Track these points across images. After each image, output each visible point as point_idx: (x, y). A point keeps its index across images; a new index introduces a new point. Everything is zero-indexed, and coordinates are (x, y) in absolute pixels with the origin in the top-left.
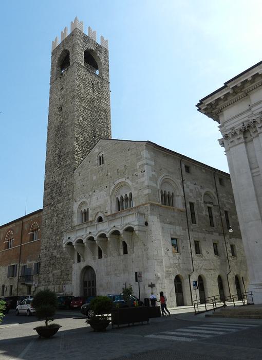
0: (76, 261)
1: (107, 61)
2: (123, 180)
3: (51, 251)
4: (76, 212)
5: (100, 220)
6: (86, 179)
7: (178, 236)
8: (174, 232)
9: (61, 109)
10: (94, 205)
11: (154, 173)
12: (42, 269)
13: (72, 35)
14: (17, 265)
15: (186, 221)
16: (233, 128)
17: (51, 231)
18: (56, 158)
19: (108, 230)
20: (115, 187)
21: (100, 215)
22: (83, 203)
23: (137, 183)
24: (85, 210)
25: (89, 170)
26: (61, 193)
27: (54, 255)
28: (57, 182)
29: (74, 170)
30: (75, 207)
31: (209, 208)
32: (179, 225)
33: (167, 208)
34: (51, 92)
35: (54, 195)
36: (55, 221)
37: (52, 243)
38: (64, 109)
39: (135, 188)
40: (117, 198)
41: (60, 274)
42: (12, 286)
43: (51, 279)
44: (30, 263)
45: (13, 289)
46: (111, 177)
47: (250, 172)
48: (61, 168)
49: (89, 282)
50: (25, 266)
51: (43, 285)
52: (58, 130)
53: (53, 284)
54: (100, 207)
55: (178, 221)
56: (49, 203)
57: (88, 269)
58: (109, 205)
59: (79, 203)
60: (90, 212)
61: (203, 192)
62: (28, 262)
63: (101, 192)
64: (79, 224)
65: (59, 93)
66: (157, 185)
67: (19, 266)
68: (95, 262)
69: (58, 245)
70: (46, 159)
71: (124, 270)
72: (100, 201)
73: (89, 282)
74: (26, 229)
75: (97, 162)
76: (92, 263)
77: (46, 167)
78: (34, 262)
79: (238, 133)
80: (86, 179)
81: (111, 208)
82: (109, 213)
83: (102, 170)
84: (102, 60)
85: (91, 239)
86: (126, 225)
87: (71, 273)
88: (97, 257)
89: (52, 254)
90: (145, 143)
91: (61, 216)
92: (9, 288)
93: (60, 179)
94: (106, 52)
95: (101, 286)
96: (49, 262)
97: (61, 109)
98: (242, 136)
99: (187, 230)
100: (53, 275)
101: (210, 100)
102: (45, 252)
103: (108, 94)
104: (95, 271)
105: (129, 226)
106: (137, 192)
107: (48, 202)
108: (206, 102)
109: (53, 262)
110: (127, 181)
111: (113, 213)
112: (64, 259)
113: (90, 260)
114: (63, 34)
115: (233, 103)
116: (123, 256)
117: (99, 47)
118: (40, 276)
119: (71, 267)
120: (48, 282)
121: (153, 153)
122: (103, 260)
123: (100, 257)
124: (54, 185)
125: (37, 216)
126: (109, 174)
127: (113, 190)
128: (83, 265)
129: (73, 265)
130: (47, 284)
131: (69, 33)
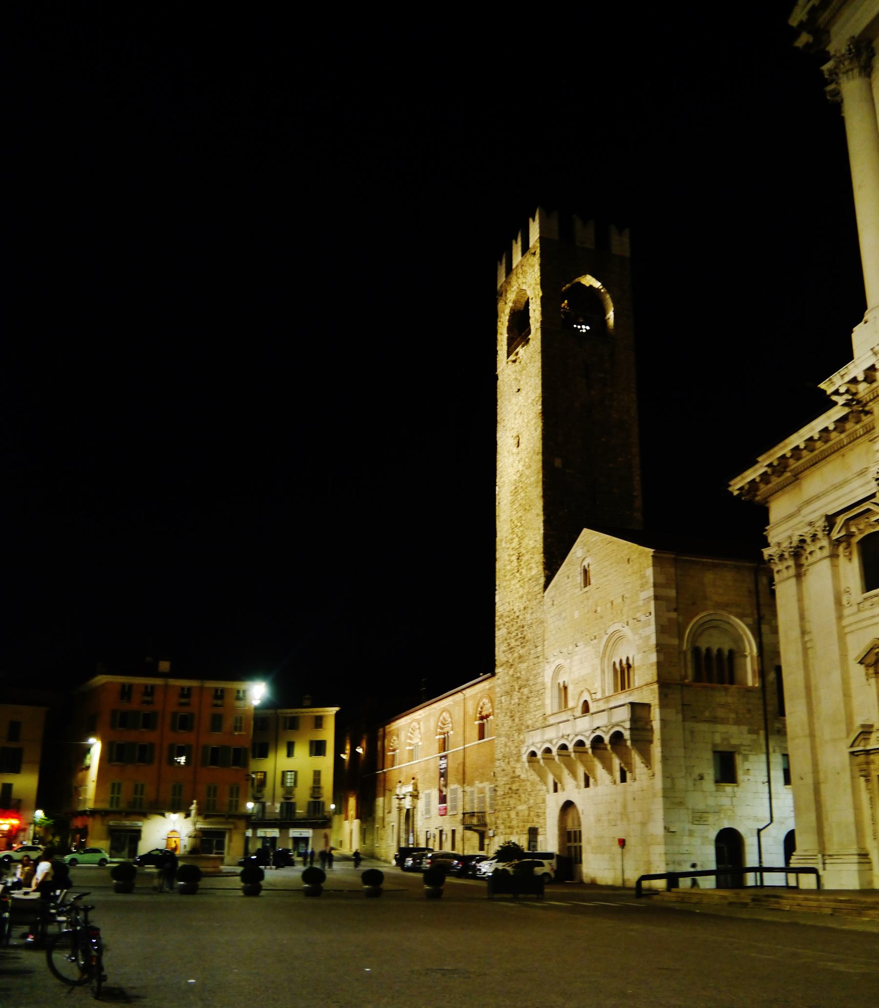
3: (512, 763)
4: (549, 685)
7: (734, 746)
8: (724, 739)
11: (673, 615)
15: (761, 712)
17: (510, 722)
18: (514, 558)
19: (587, 734)
20: (608, 641)
22: (559, 668)
25: (568, 594)
27: (517, 773)
28: (517, 614)
32: (738, 722)
33: (704, 687)
35: (513, 643)
37: (513, 748)
40: (614, 663)
41: (527, 812)
42: (453, 831)
43: (514, 823)
44: (481, 785)
46: (602, 617)
47: (799, 641)
54: (585, 680)
55: (737, 713)
56: (505, 659)
57: (568, 805)
58: (599, 678)
59: (554, 667)
64: (555, 711)
66: (681, 637)
68: (579, 793)
80: (563, 615)
82: (599, 696)
83: (588, 599)
85: (564, 747)
86: (612, 727)
88: (582, 783)
89: (514, 772)
91: (525, 691)
93: (522, 607)
95: (589, 842)
96: (510, 789)
98: (791, 563)
99: (762, 733)
101: (741, 481)
102: (503, 764)
104: (580, 812)
105: (617, 729)
108: (735, 484)
110: (627, 631)
111: (607, 695)
113: (572, 790)
119: (544, 801)
120: (509, 827)
121: (672, 570)
123: (587, 785)
124: (512, 620)
125: (487, 687)
126: (599, 609)
127: (606, 646)
130: (508, 831)
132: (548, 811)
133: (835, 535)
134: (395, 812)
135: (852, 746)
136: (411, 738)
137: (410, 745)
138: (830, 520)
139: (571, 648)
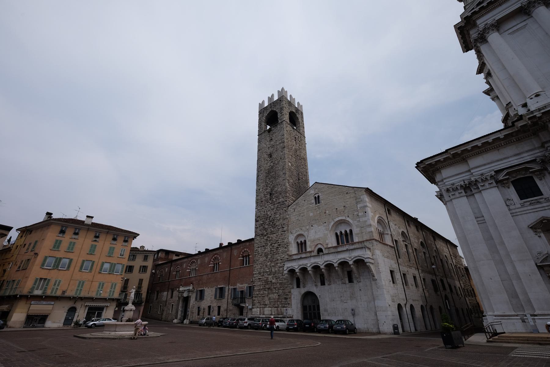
0: (295, 287)
1: (303, 121)
2: (344, 218)
4: (293, 242)
5: (320, 250)
6: (302, 215)
9: (270, 156)
10: (312, 238)
12: (255, 293)
13: (280, 100)
14: (225, 288)
16: (453, 184)
17: (265, 258)
18: (268, 196)
21: (320, 246)
23: (359, 221)
24: (301, 241)
26: (274, 226)
28: (270, 215)
29: (288, 207)
30: (291, 238)
31: (406, 245)
34: (259, 141)
35: (266, 227)
36: (269, 249)
38: (274, 156)
39: (357, 226)
40: (336, 234)
41: (277, 297)
42: (219, 307)
43: (267, 302)
45: (222, 309)
48: (273, 203)
49: (310, 306)
50: (235, 289)
51: (257, 307)
52: (269, 172)
53: (269, 307)
59: (295, 235)
60: (308, 243)
61: (400, 231)
62: (238, 285)
63: (320, 227)
65: (267, 143)
67: (229, 289)
69: (273, 270)
70: (257, 196)
71: (351, 297)
72: (321, 234)
73: (310, 306)
74: (235, 254)
75: (313, 201)
76: (314, 290)
77: (257, 203)
78: (246, 285)
79: (459, 188)
80: (302, 215)
81: (332, 242)
82: (329, 246)
84: (300, 120)
87: (290, 298)
88: (319, 284)
90: (364, 190)
92: (217, 309)
94: (302, 113)
95: (326, 310)
97: (270, 156)
100: (270, 299)
103: (305, 146)
106: (359, 229)
107: (260, 233)
109: (268, 286)
112: (281, 284)
114: (270, 99)
115: (451, 165)
116: (348, 285)
117: (297, 110)
118: (254, 298)
119: (290, 292)
122: (326, 287)
126: (327, 212)
127: (333, 226)
128: (303, 290)
129: (292, 290)
131: (276, 98)
132: (292, 296)
133: (501, 177)
134: (175, 298)
135: (541, 262)
136: (190, 267)
137: (189, 269)
138: (498, 172)
139: (307, 227)
